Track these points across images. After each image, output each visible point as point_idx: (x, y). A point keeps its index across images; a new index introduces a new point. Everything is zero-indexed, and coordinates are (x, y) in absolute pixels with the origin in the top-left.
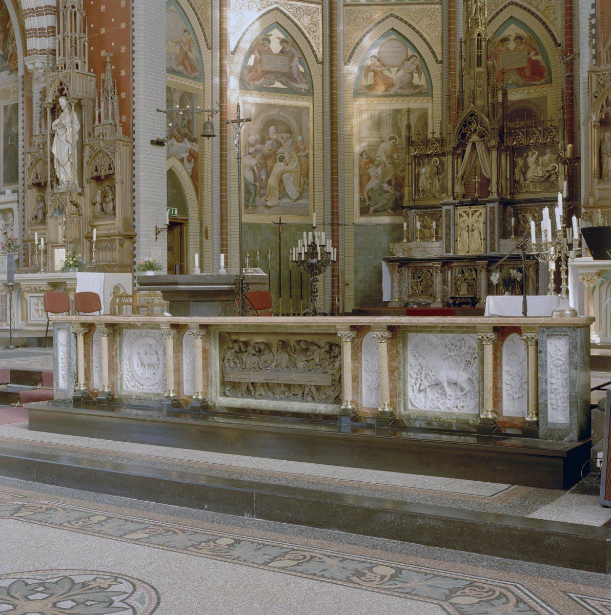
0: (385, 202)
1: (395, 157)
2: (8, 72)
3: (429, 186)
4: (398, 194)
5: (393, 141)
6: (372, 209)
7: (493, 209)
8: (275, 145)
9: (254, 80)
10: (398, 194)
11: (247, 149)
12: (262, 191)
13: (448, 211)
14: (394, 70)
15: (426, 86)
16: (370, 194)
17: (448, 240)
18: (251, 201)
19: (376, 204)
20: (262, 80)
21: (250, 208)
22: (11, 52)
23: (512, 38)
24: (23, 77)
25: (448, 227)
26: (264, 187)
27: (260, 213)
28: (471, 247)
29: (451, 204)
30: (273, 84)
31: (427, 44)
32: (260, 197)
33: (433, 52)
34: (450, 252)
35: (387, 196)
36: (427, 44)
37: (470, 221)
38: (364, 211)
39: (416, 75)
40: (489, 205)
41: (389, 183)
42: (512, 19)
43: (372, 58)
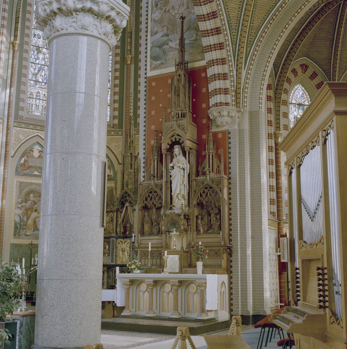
8: (33, 203)
9: (24, 170)
11: (17, 205)
12: (24, 227)
17: (113, 255)
18: (17, 232)
20: (28, 170)
21: (17, 236)
26: (26, 225)
27: (22, 239)
30: (34, 173)
31: (115, 155)
32: (23, 230)
34: (113, 262)
36: (115, 155)
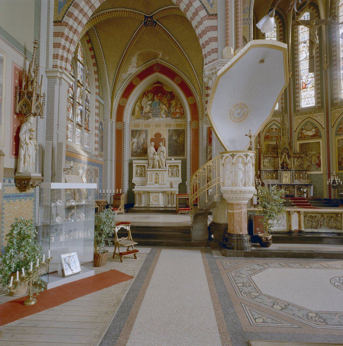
2: (171, 118)
7: (293, 172)
22: (172, 111)
23: (274, 129)
24: (190, 121)
25: (280, 176)
37: (286, 175)
40: (292, 171)
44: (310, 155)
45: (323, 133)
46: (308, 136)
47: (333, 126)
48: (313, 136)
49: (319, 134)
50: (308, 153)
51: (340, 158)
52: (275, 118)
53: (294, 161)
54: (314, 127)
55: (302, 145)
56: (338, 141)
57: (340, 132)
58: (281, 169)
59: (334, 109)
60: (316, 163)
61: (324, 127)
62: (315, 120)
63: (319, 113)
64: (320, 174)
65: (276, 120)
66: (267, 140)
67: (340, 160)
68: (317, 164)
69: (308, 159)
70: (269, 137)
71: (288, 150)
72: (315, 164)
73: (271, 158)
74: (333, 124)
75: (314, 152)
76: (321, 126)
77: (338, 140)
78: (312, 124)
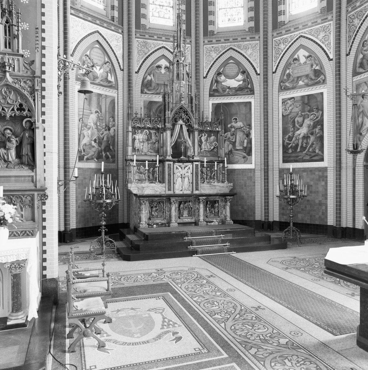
0: (93, 153)
1: (99, 125)
3: (141, 147)
4: (100, 148)
5: (97, 114)
6: (85, 157)
7: (197, 166)
10: (100, 148)
13: (169, 166)
14: (98, 68)
15: (114, 83)
16: (84, 147)
19: (88, 154)
23: (163, 67)
28: (183, 187)
29: (172, 161)
33: (119, 63)
35: (94, 149)
37: (183, 172)
38: (81, 158)
39: (109, 75)
40: (195, 163)
41: (95, 141)
42: (231, 58)
43: (86, 56)
44: (233, 129)
45: (257, 82)
46: (229, 88)
47: (276, 71)
48: (239, 91)
49: (249, 86)
50: (229, 126)
51: (287, 136)
52: (164, 43)
53: (200, 142)
54: (241, 70)
55: (217, 108)
56: (284, 101)
57: (287, 84)
58: (170, 158)
59: (280, 34)
60: (243, 147)
61: (258, 72)
62: (244, 56)
63: (251, 42)
64: (250, 170)
65: (167, 49)
66: (148, 92)
67: (287, 141)
68: (245, 149)
69: (229, 138)
70: (153, 85)
71: (187, 114)
72: (241, 148)
73: (151, 131)
74: (276, 67)
75: (239, 124)
76: (254, 69)
77: (283, 99)
78: (238, 63)
